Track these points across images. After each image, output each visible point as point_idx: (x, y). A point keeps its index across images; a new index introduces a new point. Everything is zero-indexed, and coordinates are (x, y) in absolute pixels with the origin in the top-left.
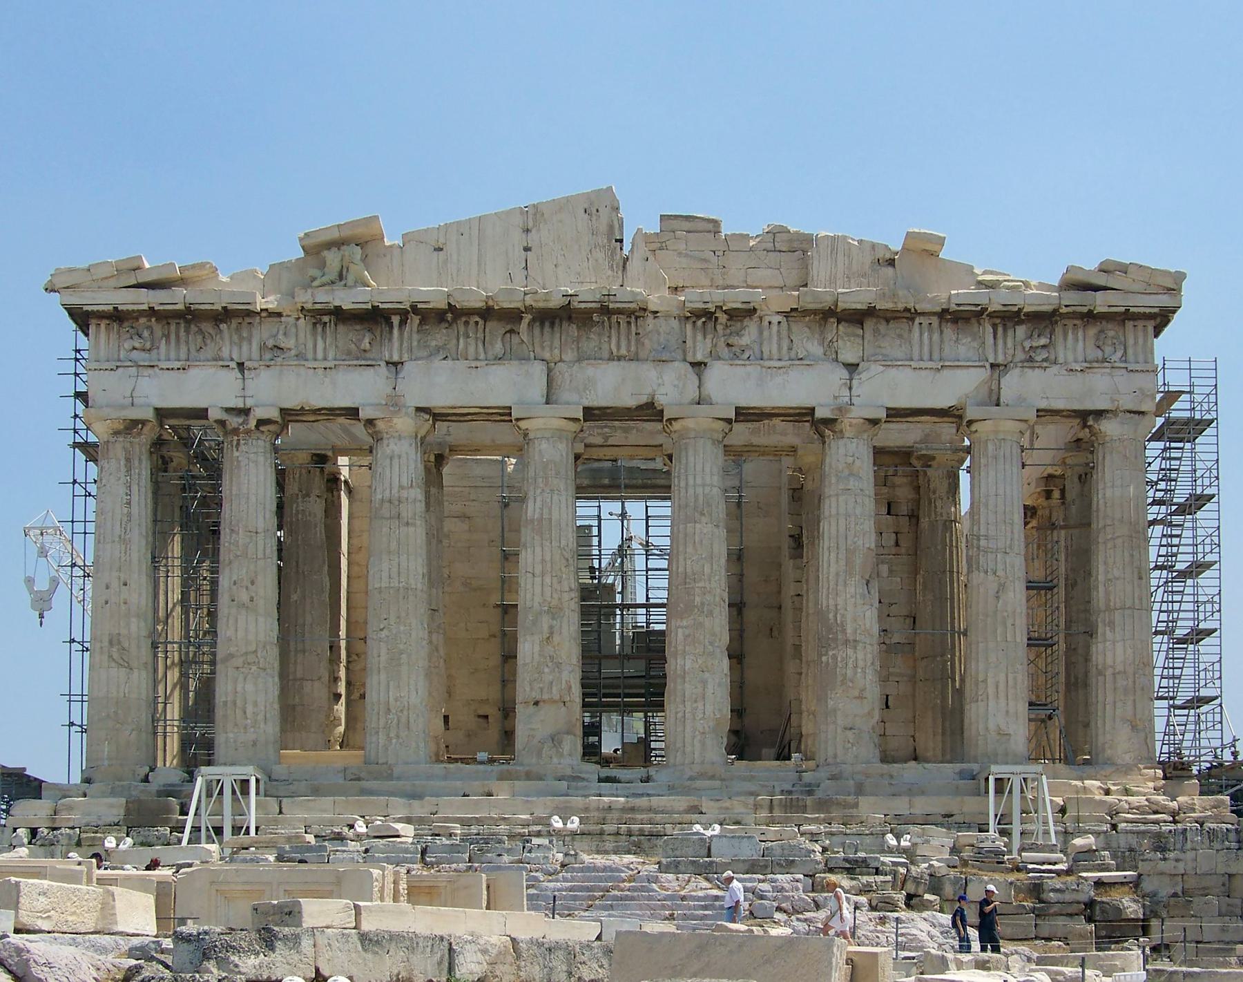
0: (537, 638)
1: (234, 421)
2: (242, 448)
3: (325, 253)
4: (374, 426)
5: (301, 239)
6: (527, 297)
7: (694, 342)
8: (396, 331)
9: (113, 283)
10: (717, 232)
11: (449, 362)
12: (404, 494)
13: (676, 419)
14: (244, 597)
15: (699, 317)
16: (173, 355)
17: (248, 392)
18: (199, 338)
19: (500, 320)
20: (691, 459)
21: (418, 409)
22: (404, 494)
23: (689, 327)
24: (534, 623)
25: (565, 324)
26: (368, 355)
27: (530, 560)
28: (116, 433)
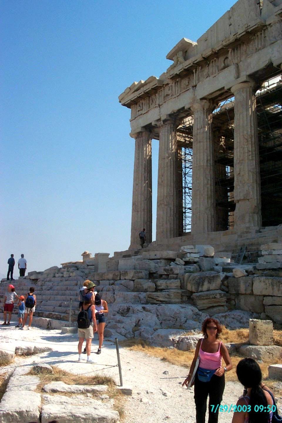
8: (194, 74)
9: (130, 93)
12: (199, 131)
21: (201, 99)
25: (242, 47)
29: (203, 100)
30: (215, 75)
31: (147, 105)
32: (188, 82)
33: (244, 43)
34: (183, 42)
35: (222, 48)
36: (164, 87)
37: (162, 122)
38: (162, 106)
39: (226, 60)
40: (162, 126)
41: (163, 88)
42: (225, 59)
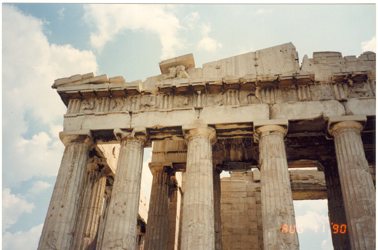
0: (274, 229)
1: (125, 134)
2: (128, 145)
3: (170, 69)
4: (189, 134)
5: (160, 64)
6: (258, 77)
7: (339, 92)
8: (199, 97)
10: (341, 56)
11: (223, 106)
12: (202, 161)
13: (333, 124)
14: (120, 211)
15: (339, 82)
16: (102, 109)
17: (132, 122)
18: (114, 104)
19: (246, 90)
20: (347, 140)
21: (210, 126)
22: (202, 161)
23: (335, 86)
24: (273, 221)
25: (276, 91)
26: (187, 106)
27: (267, 190)
28: (72, 141)
29: (211, 128)
30: (237, 106)
31: (105, 104)
32: (188, 102)
33: (278, 88)
34: (190, 57)
35: (254, 83)
36: (141, 95)
37: (133, 134)
38: (136, 115)
39: (249, 96)
40: (131, 138)
41: (140, 95)
42: (248, 95)
